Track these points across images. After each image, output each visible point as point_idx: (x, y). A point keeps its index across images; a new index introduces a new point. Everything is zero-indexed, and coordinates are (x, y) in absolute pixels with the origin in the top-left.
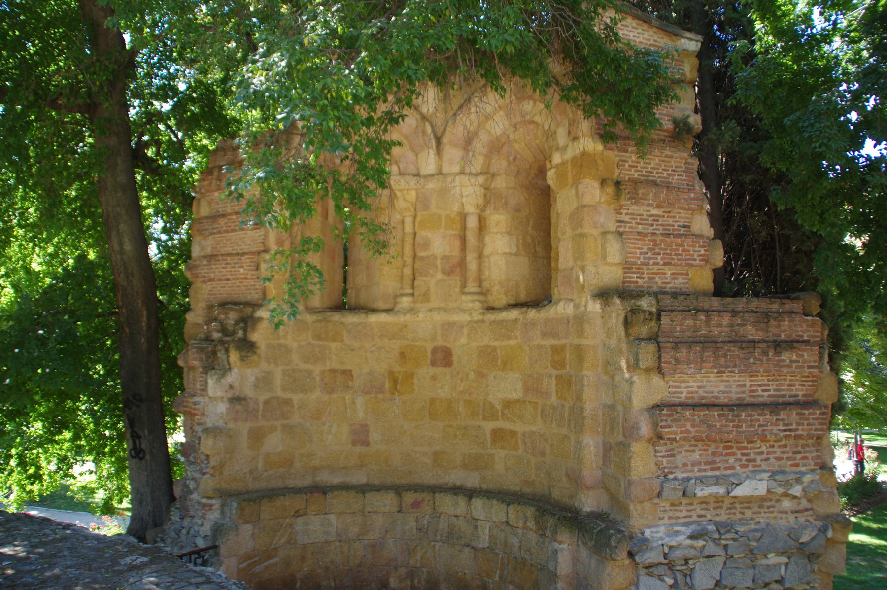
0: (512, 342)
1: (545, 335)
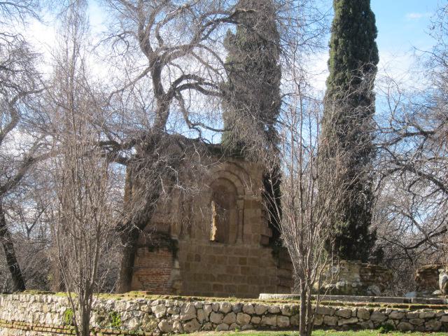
0: (222, 255)
1: (235, 254)
